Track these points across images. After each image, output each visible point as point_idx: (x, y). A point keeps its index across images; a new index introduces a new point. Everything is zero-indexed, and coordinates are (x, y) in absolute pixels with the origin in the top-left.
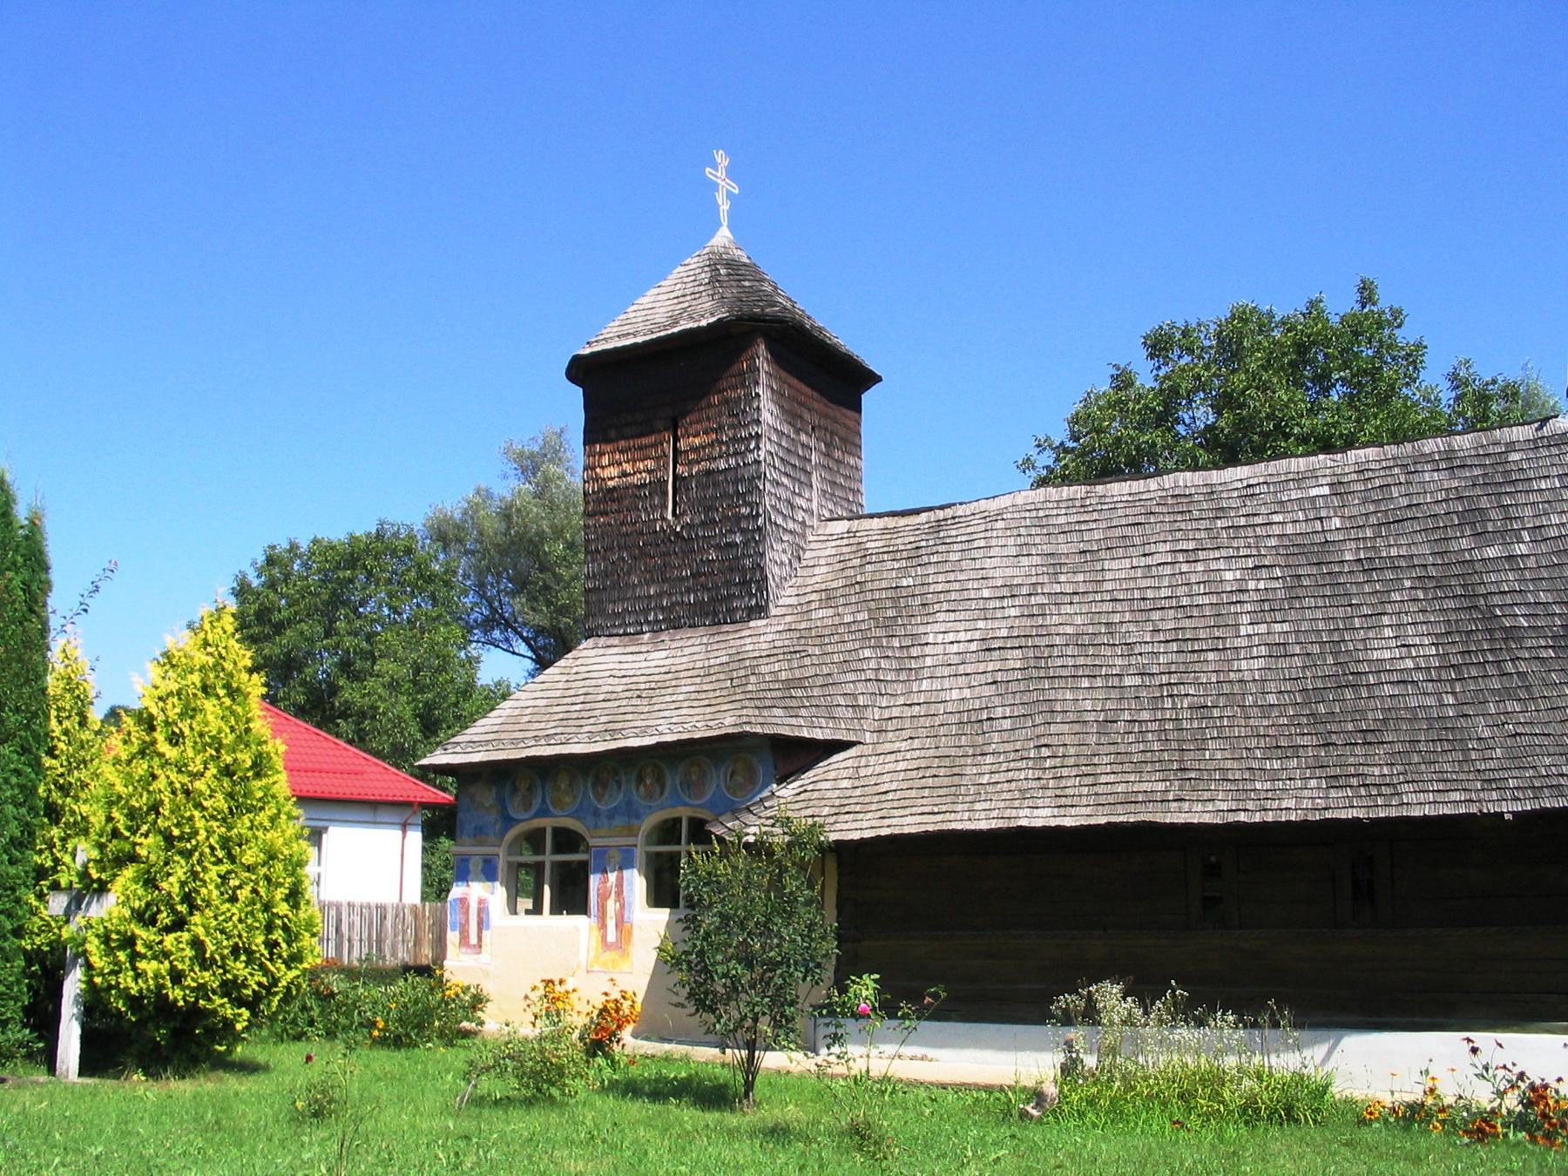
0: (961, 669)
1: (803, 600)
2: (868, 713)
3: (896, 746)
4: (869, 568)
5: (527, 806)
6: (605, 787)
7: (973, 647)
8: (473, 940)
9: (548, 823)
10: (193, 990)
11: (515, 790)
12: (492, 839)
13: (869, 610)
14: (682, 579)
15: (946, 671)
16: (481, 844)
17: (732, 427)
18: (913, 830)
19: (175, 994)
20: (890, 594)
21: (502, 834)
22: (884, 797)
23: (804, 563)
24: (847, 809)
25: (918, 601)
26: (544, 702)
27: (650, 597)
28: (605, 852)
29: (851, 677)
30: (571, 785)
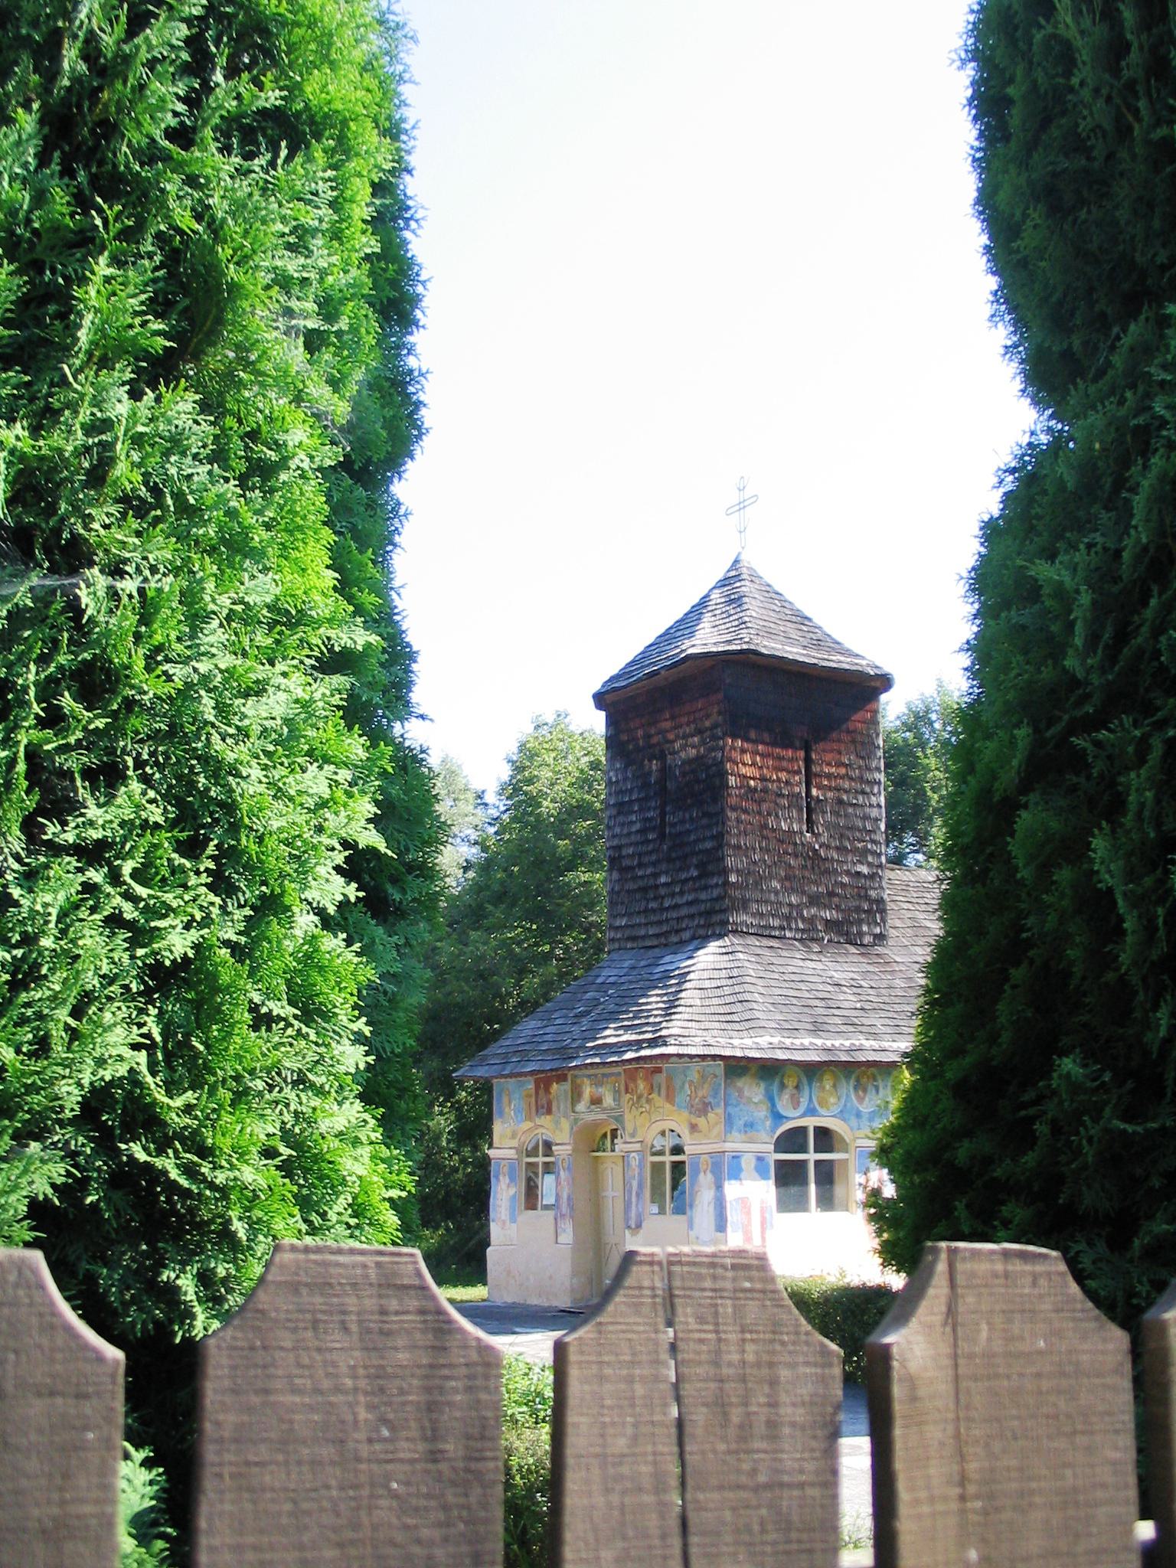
5: (796, 1105)
6: (865, 1091)
9: (811, 1122)
11: (783, 1086)
17: (860, 767)
30: (834, 1086)
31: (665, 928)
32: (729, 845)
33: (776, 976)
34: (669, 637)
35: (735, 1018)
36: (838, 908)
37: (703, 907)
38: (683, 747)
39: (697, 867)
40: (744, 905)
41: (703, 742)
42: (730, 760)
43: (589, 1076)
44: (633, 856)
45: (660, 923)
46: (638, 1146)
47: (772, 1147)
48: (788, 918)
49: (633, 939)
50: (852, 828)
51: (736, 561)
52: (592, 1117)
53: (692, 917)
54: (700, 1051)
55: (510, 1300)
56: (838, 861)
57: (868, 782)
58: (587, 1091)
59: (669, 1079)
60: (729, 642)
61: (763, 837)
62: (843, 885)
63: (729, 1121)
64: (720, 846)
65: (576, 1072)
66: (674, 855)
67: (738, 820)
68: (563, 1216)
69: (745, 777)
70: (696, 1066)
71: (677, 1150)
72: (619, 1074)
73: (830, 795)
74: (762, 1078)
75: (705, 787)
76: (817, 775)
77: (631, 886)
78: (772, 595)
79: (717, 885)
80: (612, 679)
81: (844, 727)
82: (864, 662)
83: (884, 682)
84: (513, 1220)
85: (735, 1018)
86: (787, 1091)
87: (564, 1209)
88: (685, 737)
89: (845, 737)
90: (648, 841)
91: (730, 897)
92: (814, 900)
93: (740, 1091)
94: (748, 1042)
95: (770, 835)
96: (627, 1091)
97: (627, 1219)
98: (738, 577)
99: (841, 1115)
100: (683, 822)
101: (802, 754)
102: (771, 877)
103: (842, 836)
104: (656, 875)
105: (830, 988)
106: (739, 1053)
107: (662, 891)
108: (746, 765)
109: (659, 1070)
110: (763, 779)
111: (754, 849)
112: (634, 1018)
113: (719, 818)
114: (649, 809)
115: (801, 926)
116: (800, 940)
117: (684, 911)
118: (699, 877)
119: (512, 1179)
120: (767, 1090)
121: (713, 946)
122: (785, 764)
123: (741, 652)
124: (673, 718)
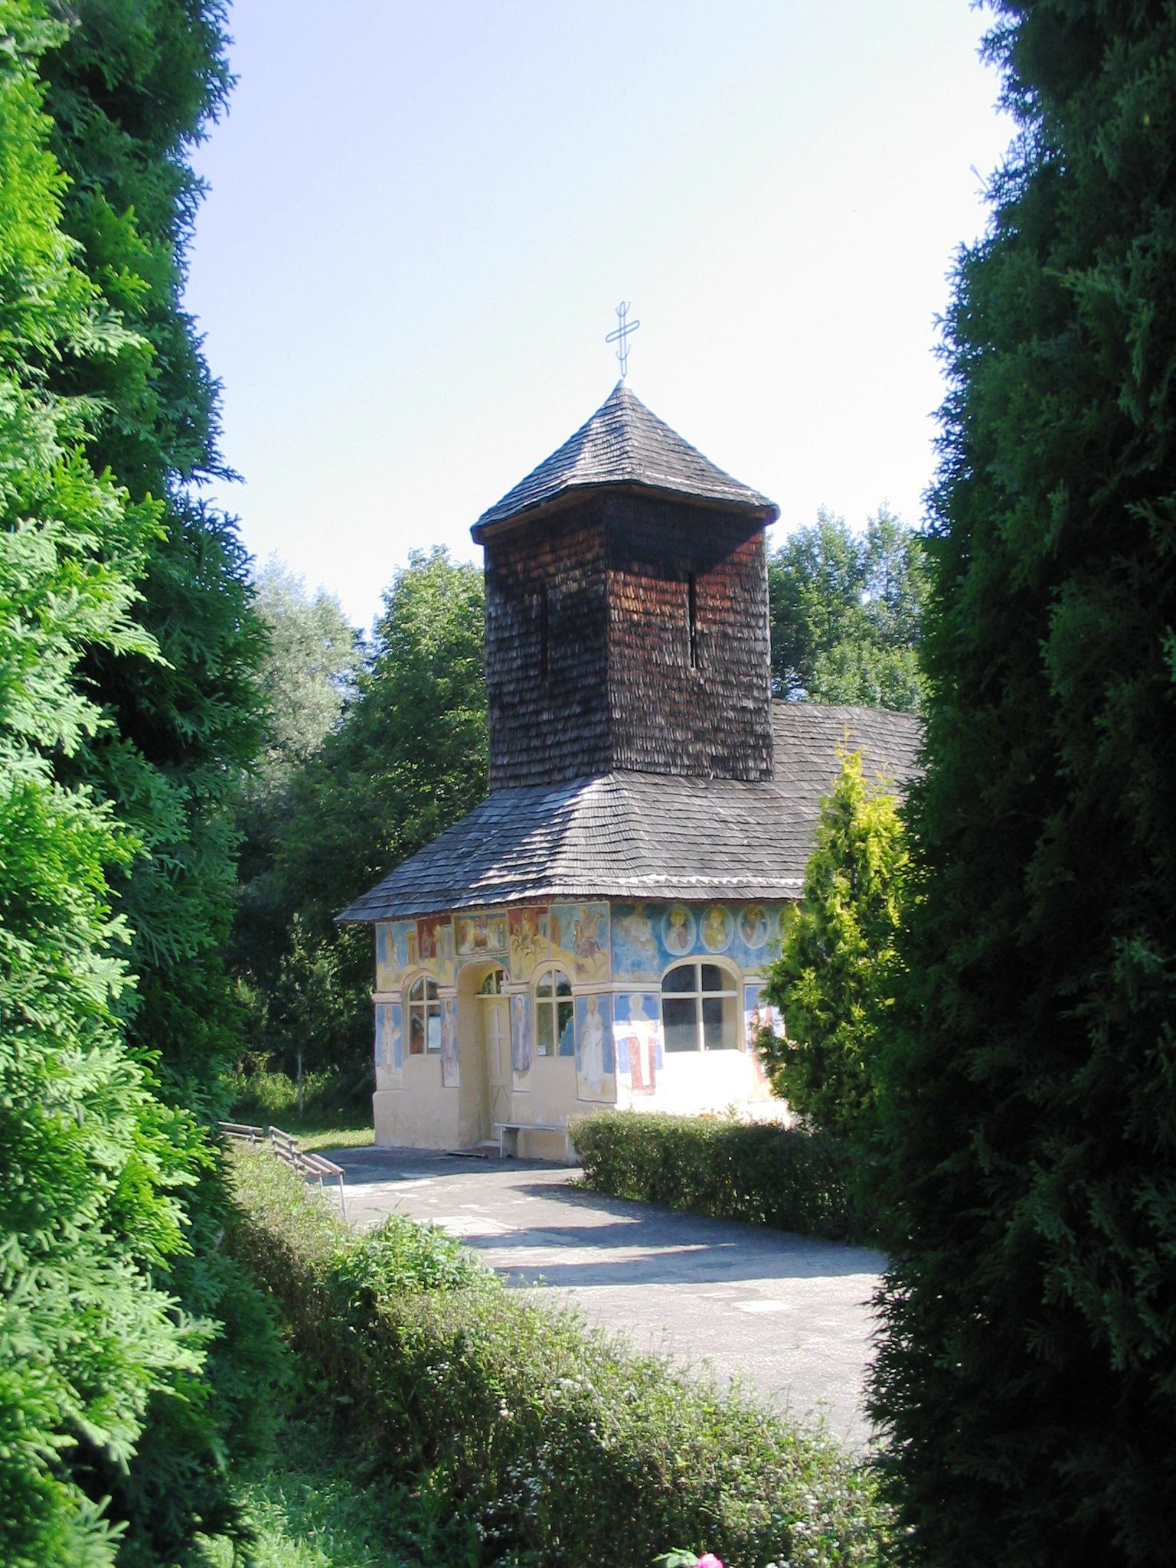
5: (683, 943)
6: (752, 927)
8: (646, 1081)
9: (698, 961)
11: (670, 925)
12: (651, 975)
17: (745, 601)
30: (722, 923)
31: (547, 767)
32: (612, 681)
33: (662, 813)
34: (549, 467)
35: (621, 856)
36: (723, 744)
37: (586, 744)
38: (564, 581)
39: (579, 703)
40: (628, 741)
41: (584, 575)
42: (612, 593)
43: (472, 918)
44: (514, 693)
45: (542, 761)
46: (523, 988)
47: (660, 986)
48: (673, 754)
49: (516, 777)
50: (738, 662)
51: (617, 390)
52: (476, 959)
53: (574, 754)
54: (586, 891)
55: (397, 1145)
56: (723, 696)
57: (753, 615)
58: (472, 933)
59: (555, 919)
60: (610, 472)
61: (647, 672)
62: (729, 721)
63: (616, 960)
64: (604, 682)
65: (461, 914)
66: (556, 692)
67: (622, 655)
68: (449, 1059)
69: (627, 610)
70: (581, 907)
71: (564, 989)
72: (503, 915)
73: (714, 628)
74: (649, 917)
75: (588, 620)
76: (701, 608)
77: (513, 724)
78: (654, 424)
79: (600, 721)
80: (490, 512)
81: (729, 559)
82: (749, 493)
83: (770, 513)
84: (399, 1064)
85: (621, 856)
86: (674, 929)
87: (451, 1052)
88: (566, 570)
89: (728, 569)
90: (529, 678)
91: (614, 733)
92: (699, 736)
93: (627, 931)
94: (634, 880)
95: (655, 670)
96: (512, 933)
97: (514, 1062)
98: (619, 406)
99: (730, 953)
100: (564, 657)
101: (686, 587)
102: (655, 713)
103: (727, 671)
104: (538, 713)
105: (717, 825)
106: (625, 893)
107: (545, 729)
108: (628, 599)
109: (543, 911)
110: (646, 613)
111: (638, 684)
112: (519, 858)
113: (600, 652)
114: (530, 645)
115: (687, 762)
116: (686, 776)
117: (566, 750)
118: (583, 714)
119: (397, 1023)
120: (654, 928)
121: (597, 784)
122: (668, 597)
123: (624, 482)
124: (553, 551)
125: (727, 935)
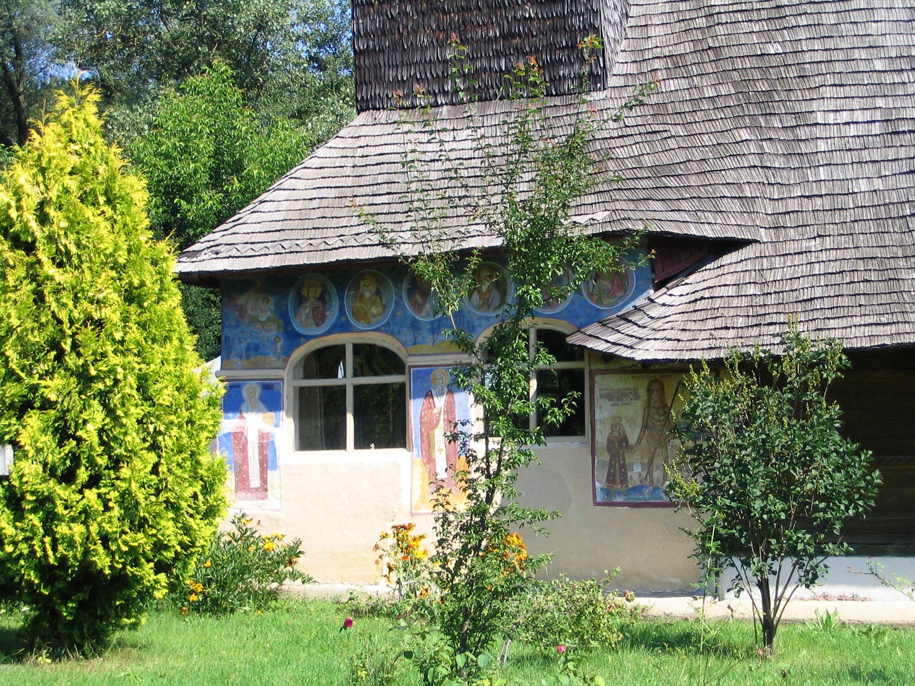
0: (865, 156)
1: (645, 68)
2: (759, 206)
3: (805, 245)
4: (721, 30)
5: (320, 319)
7: (876, 129)
8: (255, 482)
9: (347, 339)
10: (123, 554)
11: (301, 300)
13: (734, 83)
14: (489, 41)
15: (848, 158)
16: (257, 367)
18: (866, 344)
19: (102, 561)
20: (756, 62)
21: (287, 353)
22: (809, 306)
23: (632, 22)
24: (768, 319)
25: (793, 72)
26: (334, 193)
27: (445, 62)
28: (428, 373)
29: (729, 163)
30: (378, 293)
86: (308, 304)
93: (242, 311)
99: (386, 329)
120: (278, 305)
125: (384, 307)
